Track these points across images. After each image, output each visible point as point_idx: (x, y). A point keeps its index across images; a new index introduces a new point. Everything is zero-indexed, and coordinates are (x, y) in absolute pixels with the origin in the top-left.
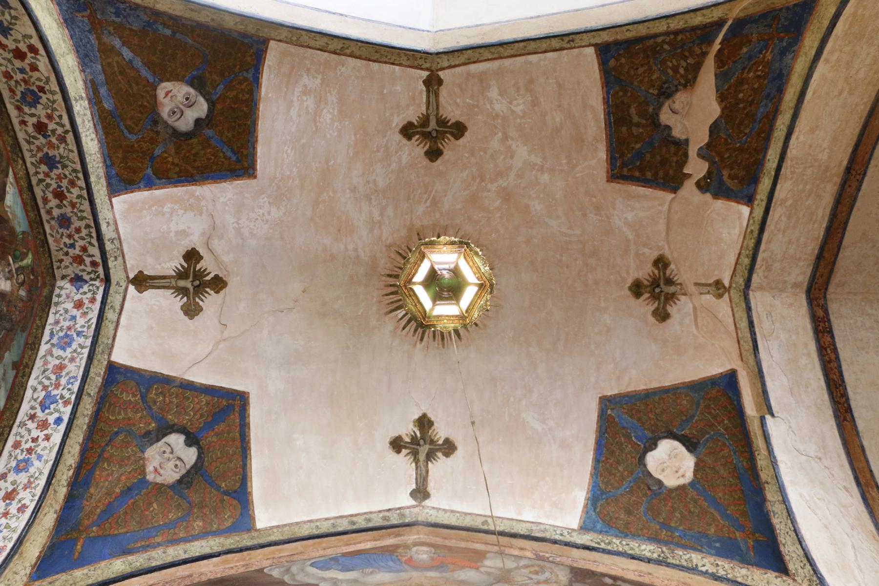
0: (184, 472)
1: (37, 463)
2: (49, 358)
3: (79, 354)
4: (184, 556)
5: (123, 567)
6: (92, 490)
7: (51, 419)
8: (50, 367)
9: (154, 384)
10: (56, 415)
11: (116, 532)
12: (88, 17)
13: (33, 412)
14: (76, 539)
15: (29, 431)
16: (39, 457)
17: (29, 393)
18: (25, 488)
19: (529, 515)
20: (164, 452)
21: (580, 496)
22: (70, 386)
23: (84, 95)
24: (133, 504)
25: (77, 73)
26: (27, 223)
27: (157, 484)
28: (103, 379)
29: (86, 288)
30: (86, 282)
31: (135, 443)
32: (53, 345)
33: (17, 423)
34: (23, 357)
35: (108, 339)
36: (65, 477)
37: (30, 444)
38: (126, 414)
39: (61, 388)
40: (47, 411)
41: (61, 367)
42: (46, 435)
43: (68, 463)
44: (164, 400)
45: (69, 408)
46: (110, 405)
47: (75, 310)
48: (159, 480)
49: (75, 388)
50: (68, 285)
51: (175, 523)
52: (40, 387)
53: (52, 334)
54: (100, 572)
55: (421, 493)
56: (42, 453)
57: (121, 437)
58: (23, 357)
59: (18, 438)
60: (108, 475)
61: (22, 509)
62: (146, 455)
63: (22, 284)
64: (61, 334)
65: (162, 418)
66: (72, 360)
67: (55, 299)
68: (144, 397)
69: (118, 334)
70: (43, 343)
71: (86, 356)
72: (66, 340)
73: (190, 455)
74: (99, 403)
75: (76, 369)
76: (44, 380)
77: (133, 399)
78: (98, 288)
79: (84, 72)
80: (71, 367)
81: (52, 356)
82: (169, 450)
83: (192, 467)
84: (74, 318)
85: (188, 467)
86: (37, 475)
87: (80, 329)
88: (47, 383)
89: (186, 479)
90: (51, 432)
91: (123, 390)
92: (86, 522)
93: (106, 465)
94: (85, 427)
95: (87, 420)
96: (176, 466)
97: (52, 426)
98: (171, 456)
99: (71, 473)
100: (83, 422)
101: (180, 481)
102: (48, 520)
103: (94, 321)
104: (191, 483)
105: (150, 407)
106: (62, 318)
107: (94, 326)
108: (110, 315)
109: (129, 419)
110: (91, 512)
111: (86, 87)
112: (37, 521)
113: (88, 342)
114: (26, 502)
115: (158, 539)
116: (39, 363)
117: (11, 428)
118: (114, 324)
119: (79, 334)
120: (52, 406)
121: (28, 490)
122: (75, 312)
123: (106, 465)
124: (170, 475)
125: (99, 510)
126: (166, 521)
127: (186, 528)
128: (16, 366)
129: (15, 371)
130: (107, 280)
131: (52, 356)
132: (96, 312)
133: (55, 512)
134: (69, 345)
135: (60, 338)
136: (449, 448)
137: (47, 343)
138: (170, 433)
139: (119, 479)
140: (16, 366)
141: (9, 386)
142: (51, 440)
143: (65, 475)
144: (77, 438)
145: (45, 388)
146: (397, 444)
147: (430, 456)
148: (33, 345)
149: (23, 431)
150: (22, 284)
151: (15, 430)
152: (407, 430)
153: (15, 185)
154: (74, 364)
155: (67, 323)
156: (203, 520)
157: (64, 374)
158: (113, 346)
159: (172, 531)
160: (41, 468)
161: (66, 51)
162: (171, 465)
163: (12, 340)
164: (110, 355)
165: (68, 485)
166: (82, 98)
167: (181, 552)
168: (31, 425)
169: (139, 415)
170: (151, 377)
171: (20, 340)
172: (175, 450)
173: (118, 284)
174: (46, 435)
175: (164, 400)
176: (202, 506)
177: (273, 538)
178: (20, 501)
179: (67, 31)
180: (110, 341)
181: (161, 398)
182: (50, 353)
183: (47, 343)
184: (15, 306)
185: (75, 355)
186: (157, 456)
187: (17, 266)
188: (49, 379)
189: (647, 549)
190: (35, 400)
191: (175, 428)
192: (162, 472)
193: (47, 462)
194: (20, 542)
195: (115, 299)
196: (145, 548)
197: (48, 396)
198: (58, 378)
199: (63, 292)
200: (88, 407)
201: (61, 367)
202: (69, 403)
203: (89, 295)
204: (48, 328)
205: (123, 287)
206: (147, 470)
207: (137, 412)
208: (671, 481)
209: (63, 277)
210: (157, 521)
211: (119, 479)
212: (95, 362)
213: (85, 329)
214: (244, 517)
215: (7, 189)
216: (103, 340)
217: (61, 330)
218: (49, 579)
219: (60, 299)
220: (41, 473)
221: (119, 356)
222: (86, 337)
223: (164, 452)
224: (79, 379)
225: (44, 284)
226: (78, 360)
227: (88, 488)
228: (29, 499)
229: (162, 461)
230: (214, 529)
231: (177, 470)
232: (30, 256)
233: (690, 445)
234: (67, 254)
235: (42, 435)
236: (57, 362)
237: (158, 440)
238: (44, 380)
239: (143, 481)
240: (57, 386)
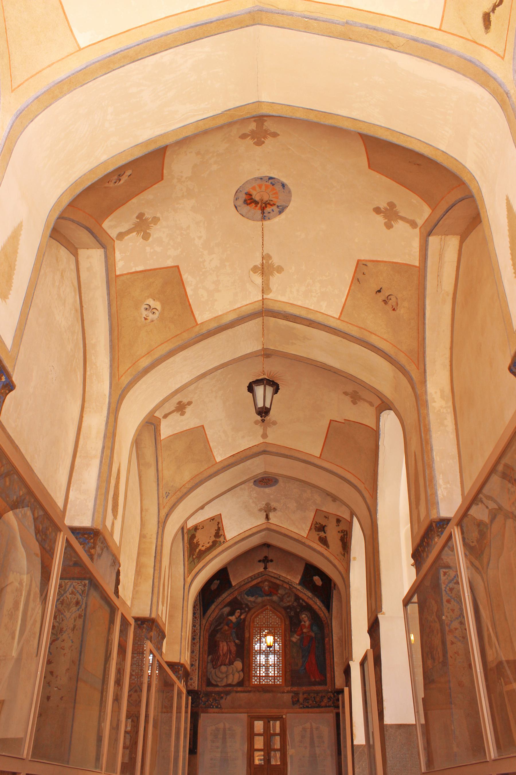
19: (289, 577)
21: (300, 577)
55: (265, 568)
73: (219, 581)
136: (272, 561)
146: (260, 561)
147: (268, 562)
152: (262, 558)
177: (237, 588)
189: (310, 594)
208: (317, 583)
214: (230, 585)
233: (322, 580)
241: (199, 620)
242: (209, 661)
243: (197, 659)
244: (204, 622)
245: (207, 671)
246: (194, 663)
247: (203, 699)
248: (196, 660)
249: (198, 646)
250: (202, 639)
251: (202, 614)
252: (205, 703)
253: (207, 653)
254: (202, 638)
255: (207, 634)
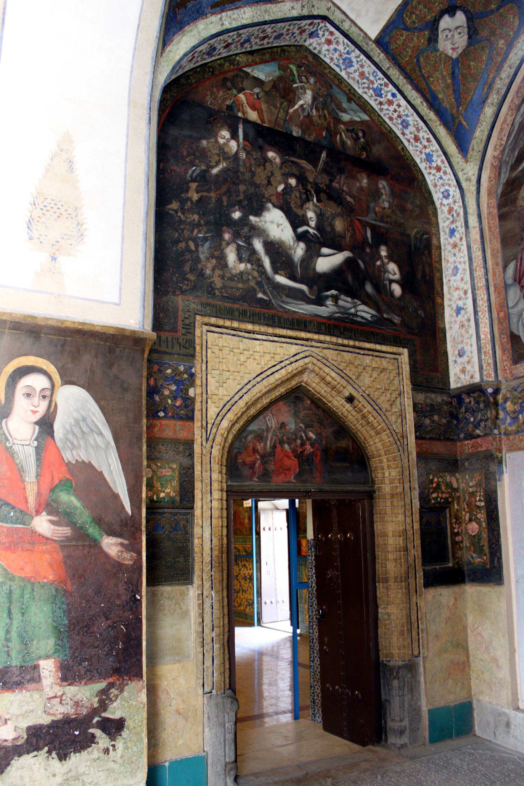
0: (466, 30)
1: (408, 119)
2: (351, 76)
3: (361, 61)
4: (512, 71)
5: (491, 110)
6: (440, 96)
7: (390, 97)
8: (357, 78)
9: (403, 17)
10: (389, 95)
11: (470, 97)
12: (179, 9)
13: (378, 101)
14: (460, 123)
15: (388, 109)
16: (407, 116)
17: (365, 96)
18: (418, 132)
20: (447, 36)
22: (377, 78)
23: (219, 16)
24: (462, 76)
25: (208, 21)
26: (273, 63)
27: (461, 53)
28: (383, 52)
29: (321, 33)
30: (317, 30)
31: (430, 52)
32: (345, 69)
33: (379, 111)
34: (344, 92)
35: (360, 35)
36: (426, 109)
37: (396, 115)
38: (410, 48)
39: (375, 82)
40: (383, 96)
41: (362, 74)
42: (397, 105)
43: (419, 103)
44: (416, 15)
45: (390, 86)
46: (399, 55)
47: (331, 46)
48: (460, 51)
49: (380, 75)
50: (311, 40)
51: (491, 58)
52: (366, 90)
53: (338, 66)
54: (484, 123)
56: (405, 113)
57: (422, 60)
58: (344, 92)
59: (388, 116)
60: (438, 81)
61: (428, 140)
62: (441, 50)
63: (307, 79)
64: (341, 61)
65: (426, 23)
66: (362, 66)
67: (316, 52)
68: (406, 29)
69: (360, 25)
70: (339, 73)
71: (365, 58)
72: (347, 61)
74: (395, 63)
75: (369, 68)
76: (363, 86)
77: (404, 38)
78: (325, 26)
79: (206, 14)
80: (366, 70)
81: (351, 73)
82: (447, 31)
83: (468, 22)
84: (335, 50)
85: (465, 25)
86: (416, 123)
87: (346, 51)
88: (366, 85)
89: (471, 32)
90: (397, 102)
91: (395, 41)
92: (454, 111)
93: (431, 79)
94: (405, 80)
95: (401, 77)
96: (460, 33)
97: (394, 100)
98: (452, 33)
99: (425, 104)
100: (401, 81)
101: (470, 37)
102: (442, 132)
103: (346, 41)
104: (476, 30)
105: (415, 28)
106: (330, 55)
107: (349, 43)
108: (346, 26)
109: (414, 47)
110: (451, 104)
111: (215, 13)
112: (440, 139)
113: (357, 52)
114: (426, 136)
115: (491, 76)
116: (351, 82)
117: (379, 115)
118: (352, 25)
119: (348, 53)
120: (383, 92)
121: (421, 132)
122: (332, 47)
123: (431, 79)
124: (461, 41)
125: (453, 100)
126: (485, 62)
127: (497, 54)
128: (350, 100)
129: (352, 102)
130: (324, 18)
131: (351, 73)
132: (341, 36)
133: (440, 125)
134: (351, 62)
135: (343, 64)
137: (341, 71)
138: (438, 24)
139: (444, 77)
140: (350, 100)
141: (359, 109)
142: (401, 104)
143: (424, 109)
144: (408, 89)
145: (368, 88)
148: (340, 80)
149: (385, 112)
150: (307, 79)
151: (382, 114)
153: (252, 68)
154: (365, 67)
155: (336, 55)
156: (502, 38)
157: (367, 75)
158: (365, 34)
159: (492, 64)
160: (413, 119)
161: (196, 30)
162: (457, 36)
163: (336, 98)
164: (370, 39)
165: (430, 109)
166: (221, 18)
167: (509, 70)
168: (385, 107)
169: (415, 39)
170: (397, 15)
171: (336, 90)
172: (450, 28)
173: (328, 9)
174: (397, 105)
175: (416, 15)
176: (493, 33)
178: (423, 138)
179: (186, 28)
180: (362, 34)
181: (414, 16)
182: (348, 74)
183: (341, 71)
184: (320, 90)
185: (360, 63)
186: (446, 42)
187: (298, 81)
188: (364, 83)
190: (372, 96)
191: (437, 17)
192: (456, 46)
193: (412, 115)
194: (445, 154)
195: (336, 17)
196: (490, 87)
197: (374, 90)
198: (367, 79)
199: (314, 45)
200: (394, 73)
201: (362, 74)
202: (388, 84)
203: (327, 33)
204: (332, 65)
205: (332, 5)
206: (450, 55)
207: (412, 39)
209: (305, 41)
210: (481, 68)
211: (444, 77)
212: (371, 54)
213: (348, 49)
215: (256, 75)
216: (359, 40)
217: (338, 60)
218: (470, 149)
219: (318, 49)
220: (416, 121)
221: (373, 33)
222: (354, 51)
223: (447, 36)
224: (377, 70)
225: (306, 58)
226: (364, 64)
227: (437, 98)
228: (425, 134)
229: (450, 41)
230: (512, 36)
231: (462, 34)
232: (291, 66)
234: (295, 37)
235: (395, 106)
236: (357, 73)
237: (437, 35)
238: (363, 86)
239: (455, 62)
240: (372, 83)
241: (449, 170)
242: (510, 281)
243: (468, 287)
244: (470, 170)
245: (508, 316)
246: (460, 303)
247: (509, 405)
248: (465, 293)
249: (464, 248)
250: (473, 221)
251: (452, 148)
252: (515, 419)
253: (500, 260)
254: (473, 221)
255: (494, 202)
